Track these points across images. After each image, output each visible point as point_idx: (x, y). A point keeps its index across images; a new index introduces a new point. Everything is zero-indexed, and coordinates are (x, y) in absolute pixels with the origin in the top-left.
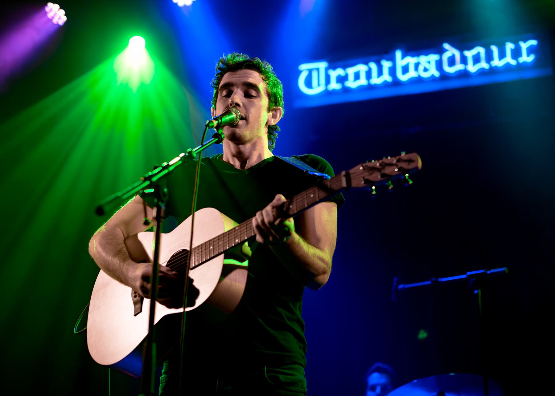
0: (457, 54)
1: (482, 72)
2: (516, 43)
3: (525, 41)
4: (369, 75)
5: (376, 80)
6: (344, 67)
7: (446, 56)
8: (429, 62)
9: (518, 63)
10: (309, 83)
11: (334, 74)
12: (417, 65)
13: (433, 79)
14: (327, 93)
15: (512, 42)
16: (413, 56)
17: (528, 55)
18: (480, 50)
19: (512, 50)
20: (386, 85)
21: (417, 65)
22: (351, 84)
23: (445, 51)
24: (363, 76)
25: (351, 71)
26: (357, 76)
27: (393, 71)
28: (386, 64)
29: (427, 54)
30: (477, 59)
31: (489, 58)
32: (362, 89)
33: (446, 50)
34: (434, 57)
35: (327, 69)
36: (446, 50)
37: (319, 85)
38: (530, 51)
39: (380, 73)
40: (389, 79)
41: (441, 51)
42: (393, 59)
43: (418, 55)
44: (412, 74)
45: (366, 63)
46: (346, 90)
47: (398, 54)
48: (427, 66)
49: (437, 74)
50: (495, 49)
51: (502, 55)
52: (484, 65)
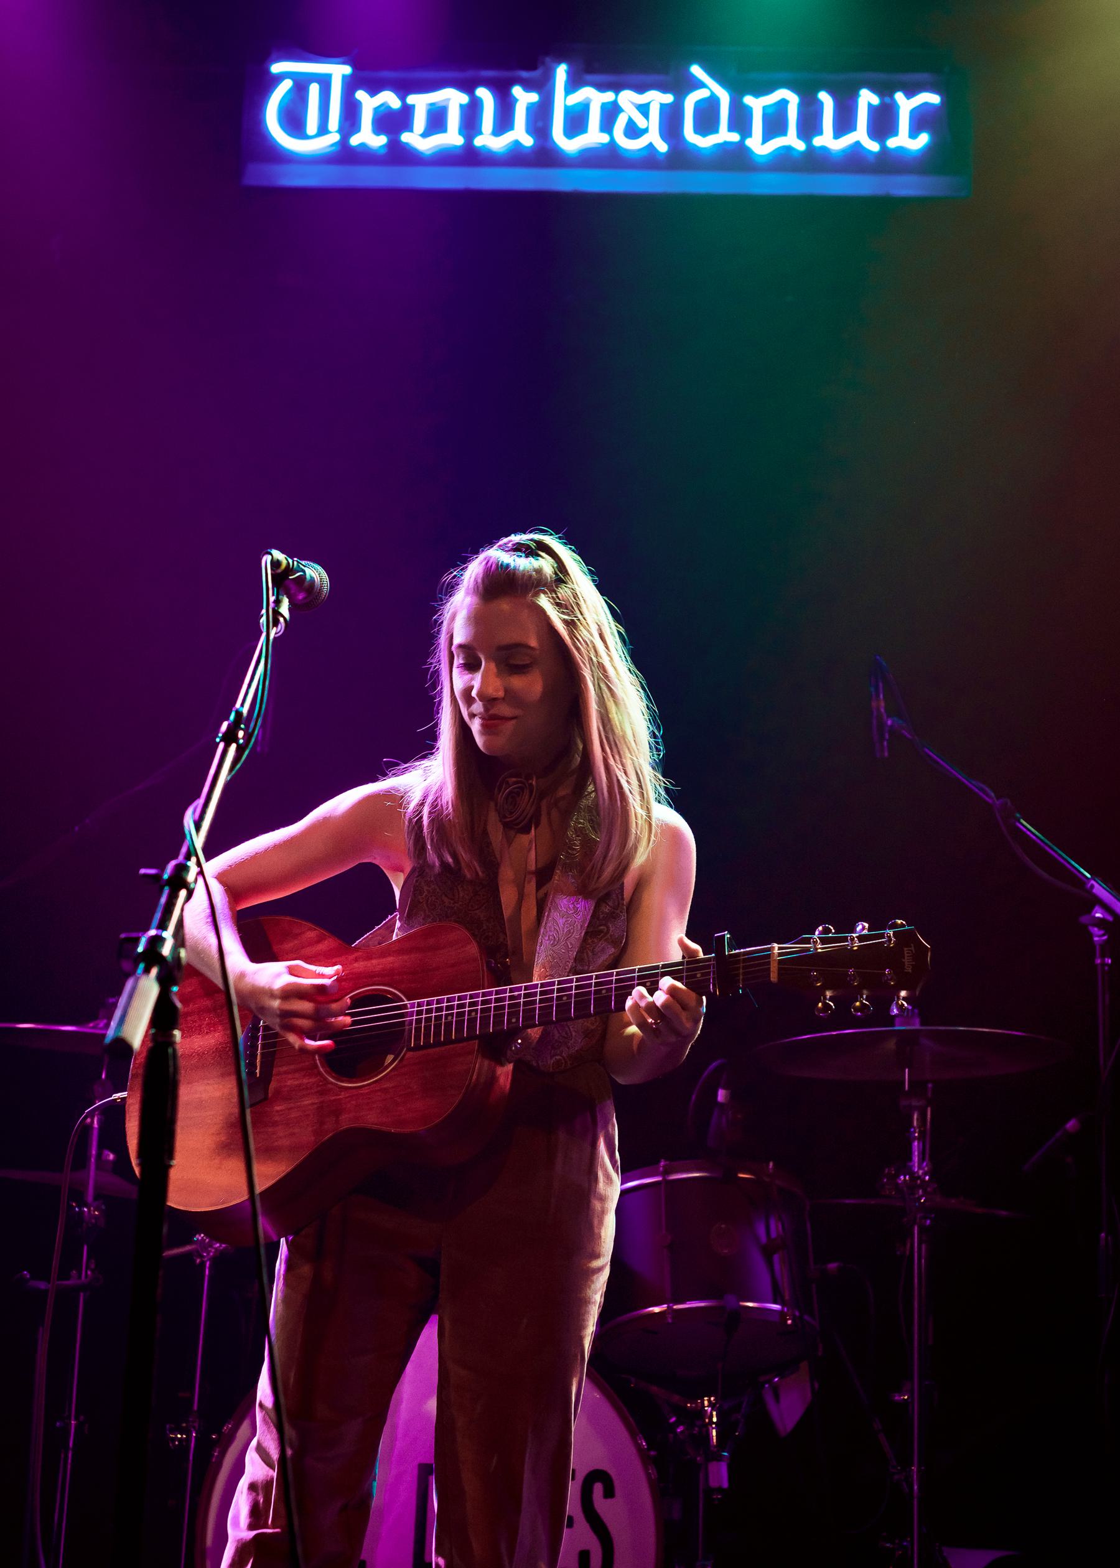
0: (724, 98)
1: (784, 161)
2: (885, 90)
3: (910, 93)
4: (471, 119)
5: (488, 140)
6: (404, 88)
7: (690, 102)
8: (644, 110)
9: (884, 149)
10: (294, 122)
11: (369, 103)
12: (610, 114)
13: (649, 160)
14: (346, 155)
15: (874, 89)
16: (601, 87)
17: (914, 133)
19: (872, 110)
21: (610, 114)
22: (415, 139)
24: (454, 119)
25: (421, 102)
27: (540, 119)
28: (524, 98)
29: (641, 89)
30: (775, 124)
31: (809, 125)
32: (445, 159)
33: (699, 85)
34: (658, 99)
35: (351, 86)
36: (699, 85)
37: (323, 130)
38: (921, 120)
39: (504, 122)
40: (528, 141)
41: (682, 85)
42: (543, 85)
43: (617, 88)
44: (593, 137)
45: (468, 87)
46: (399, 155)
47: (561, 72)
48: (641, 122)
49: (662, 147)
51: (844, 123)
52: (792, 140)
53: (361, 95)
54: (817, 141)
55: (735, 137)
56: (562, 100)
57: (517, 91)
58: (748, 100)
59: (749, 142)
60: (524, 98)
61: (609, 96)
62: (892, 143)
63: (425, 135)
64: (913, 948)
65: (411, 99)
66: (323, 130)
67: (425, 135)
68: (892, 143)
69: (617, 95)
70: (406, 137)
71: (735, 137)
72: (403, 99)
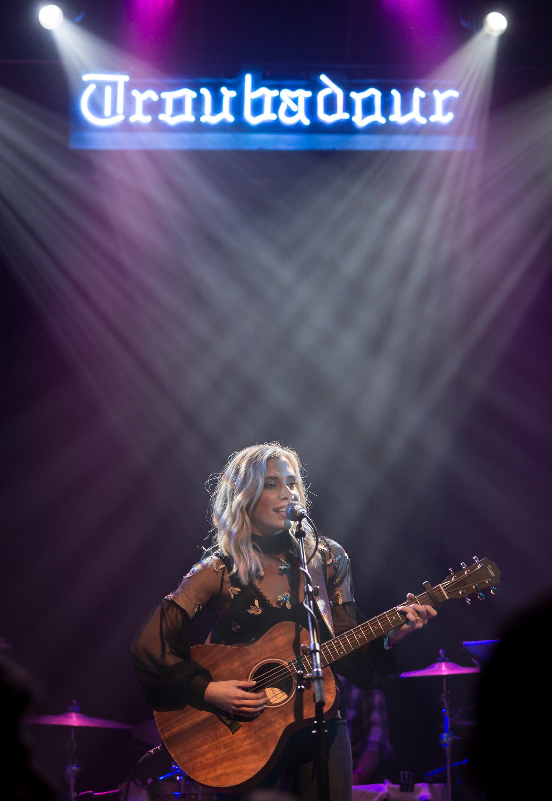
0: (340, 94)
1: (373, 129)
2: (428, 89)
7: (321, 95)
8: (296, 101)
12: (277, 103)
13: (298, 128)
16: (271, 87)
18: (375, 93)
19: (422, 100)
20: (223, 127)
21: (277, 103)
23: (323, 86)
24: (188, 106)
25: (169, 97)
26: (179, 106)
28: (228, 94)
31: (387, 108)
34: (303, 94)
35: (129, 87)
37: (114, 112)
38: (448, 106)
39: (217, 107)
40: (231, 119)
41: (317, 87)
42: (238, 87)
43: (280, 88)
44: (267, 116)
45: (196, 87)
47: (248, 78)
48: (294, 108)
49: (306, 122)
50: (395, 93)
51: (406, 108)
52: (378, 117)
53: (135, 93)
54: (392, 118)
55: (346, 116)
56: (250, 95)
57: (224, 90)
58: (353, 95)
59: (354, 119)
60: (228, 94)
61: (275, 93)
62: (433, 119)
63: (173, 115)
64: (490, 566)
65: (164, 95)
66: (114, 112)
67: (173, 115)
68: (433, 119)
69: (280, 92)
70: (161, 117)
71: (346, 116)
72: (159, 94)
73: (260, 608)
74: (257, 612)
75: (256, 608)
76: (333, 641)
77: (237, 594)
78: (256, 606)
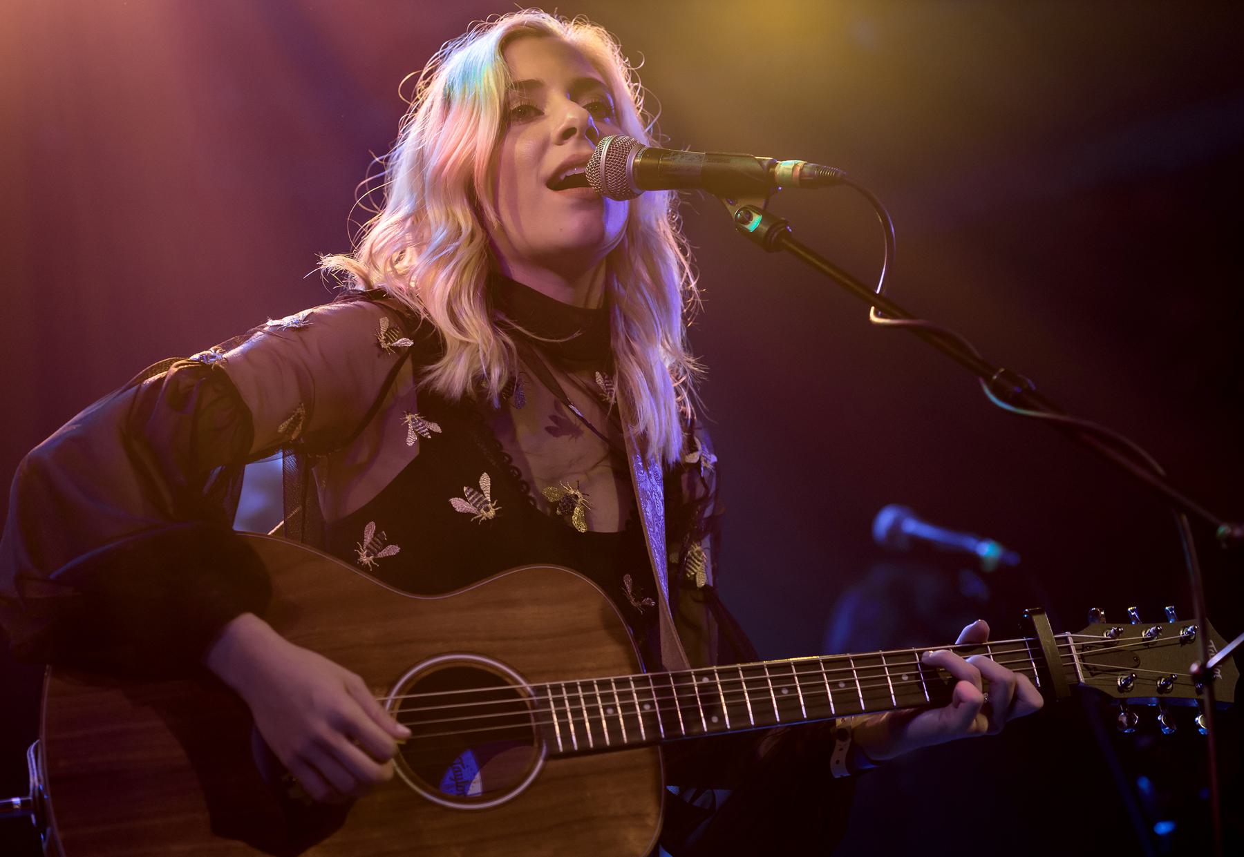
73: (492, 502)
74: (482, 510)
75: (481, 499)
76: (699, 676)
77: (429, 437)
78: (481, 492)
